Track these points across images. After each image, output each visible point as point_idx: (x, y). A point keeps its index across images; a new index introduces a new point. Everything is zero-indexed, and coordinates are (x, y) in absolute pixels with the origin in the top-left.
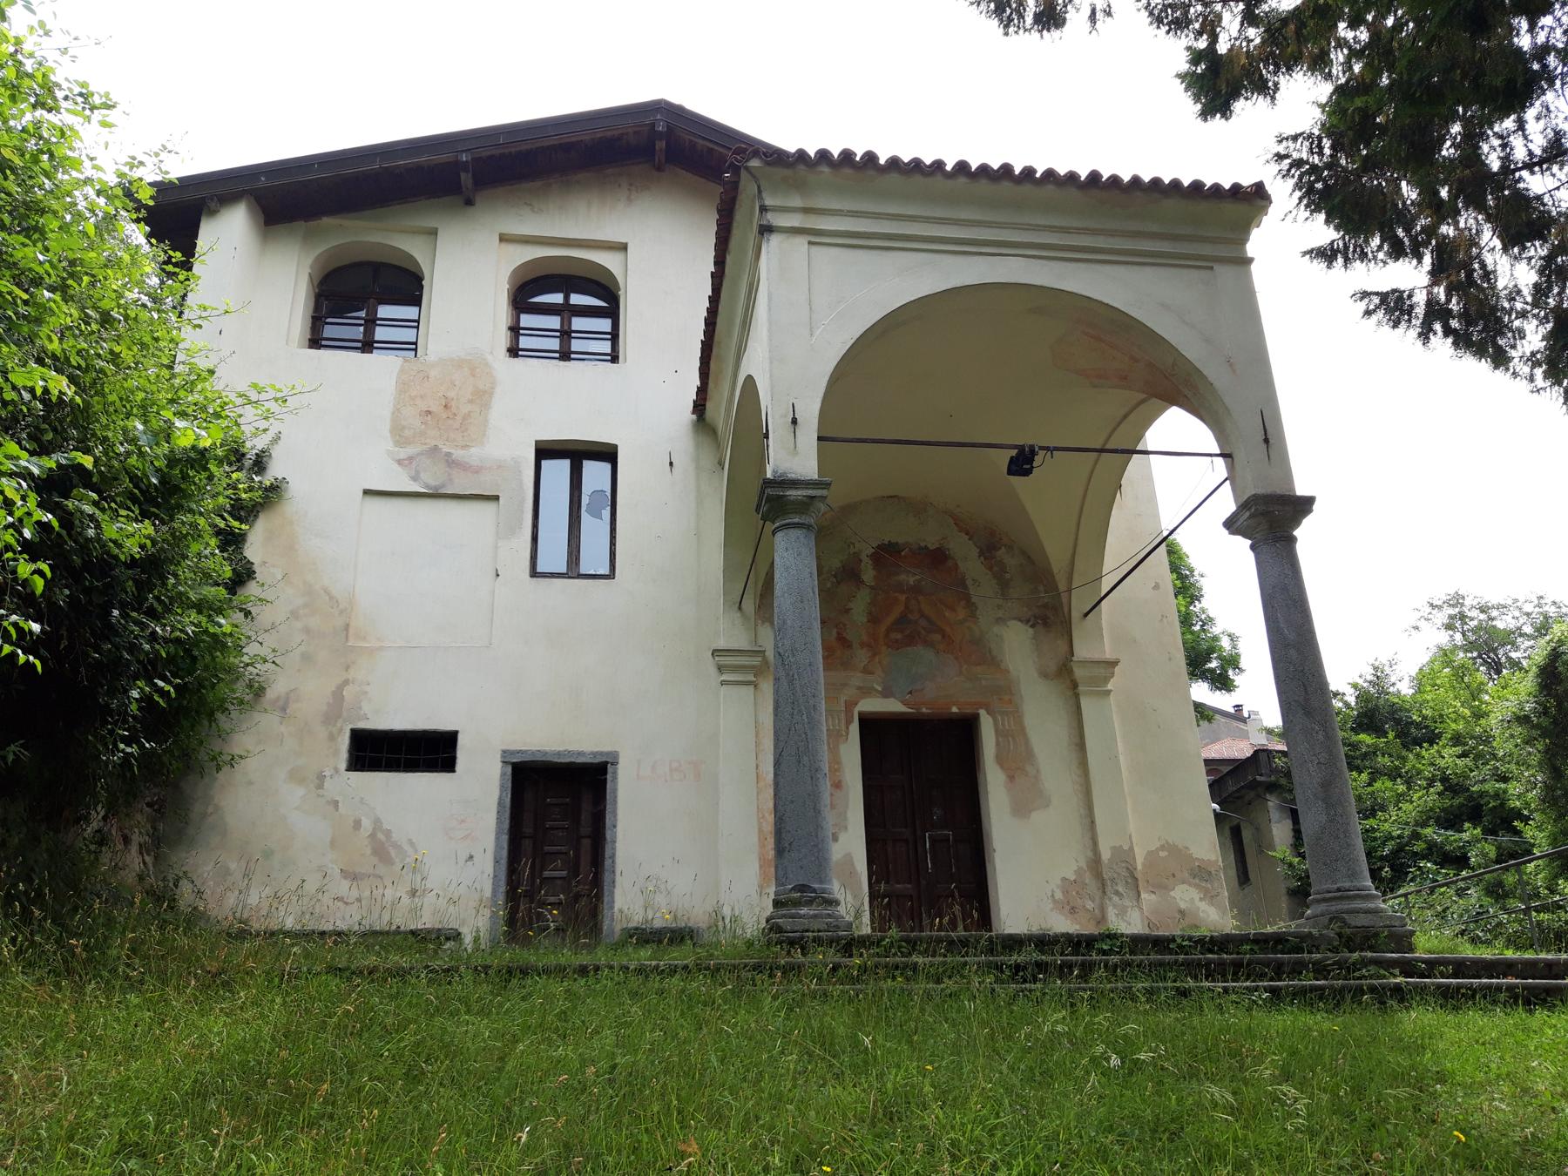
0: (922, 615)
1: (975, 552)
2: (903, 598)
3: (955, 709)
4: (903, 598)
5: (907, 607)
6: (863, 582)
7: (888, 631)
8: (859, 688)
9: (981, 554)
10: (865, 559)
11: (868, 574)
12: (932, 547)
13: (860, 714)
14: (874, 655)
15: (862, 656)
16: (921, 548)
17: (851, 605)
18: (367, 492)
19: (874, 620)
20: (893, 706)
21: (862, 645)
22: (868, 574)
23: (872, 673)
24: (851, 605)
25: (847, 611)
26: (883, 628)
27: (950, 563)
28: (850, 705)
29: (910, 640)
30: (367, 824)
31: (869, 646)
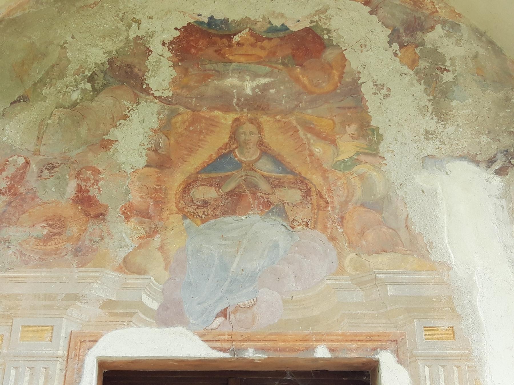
0: (265, 151)
1: (382, 34)
2: (228, 119)
3: (322, 352)
4: (228, 119)
5: (234, 136)
6: (147, 91)
7: (188, 186)
8: (108, 304)
9: (395, 37)
10: (156, 46)
11: (162, 75)
12: (294, 27)
13: (102, 364)
14: (152, 233)
15: (123, 234)
16: (273, 30)
17: (115, 134)
18: (12, 103)
19: (161, 162)
20: (181, 345)
21: (129, 212)
22: (162, 75)
23: (140, 271)
24: (115, 134)
25: (106, 145)
26: (176, 180)
27: (329, 55)
28: (79, 344)
29: (235, 202)
30: (105, 213)
31: (144, 214)
